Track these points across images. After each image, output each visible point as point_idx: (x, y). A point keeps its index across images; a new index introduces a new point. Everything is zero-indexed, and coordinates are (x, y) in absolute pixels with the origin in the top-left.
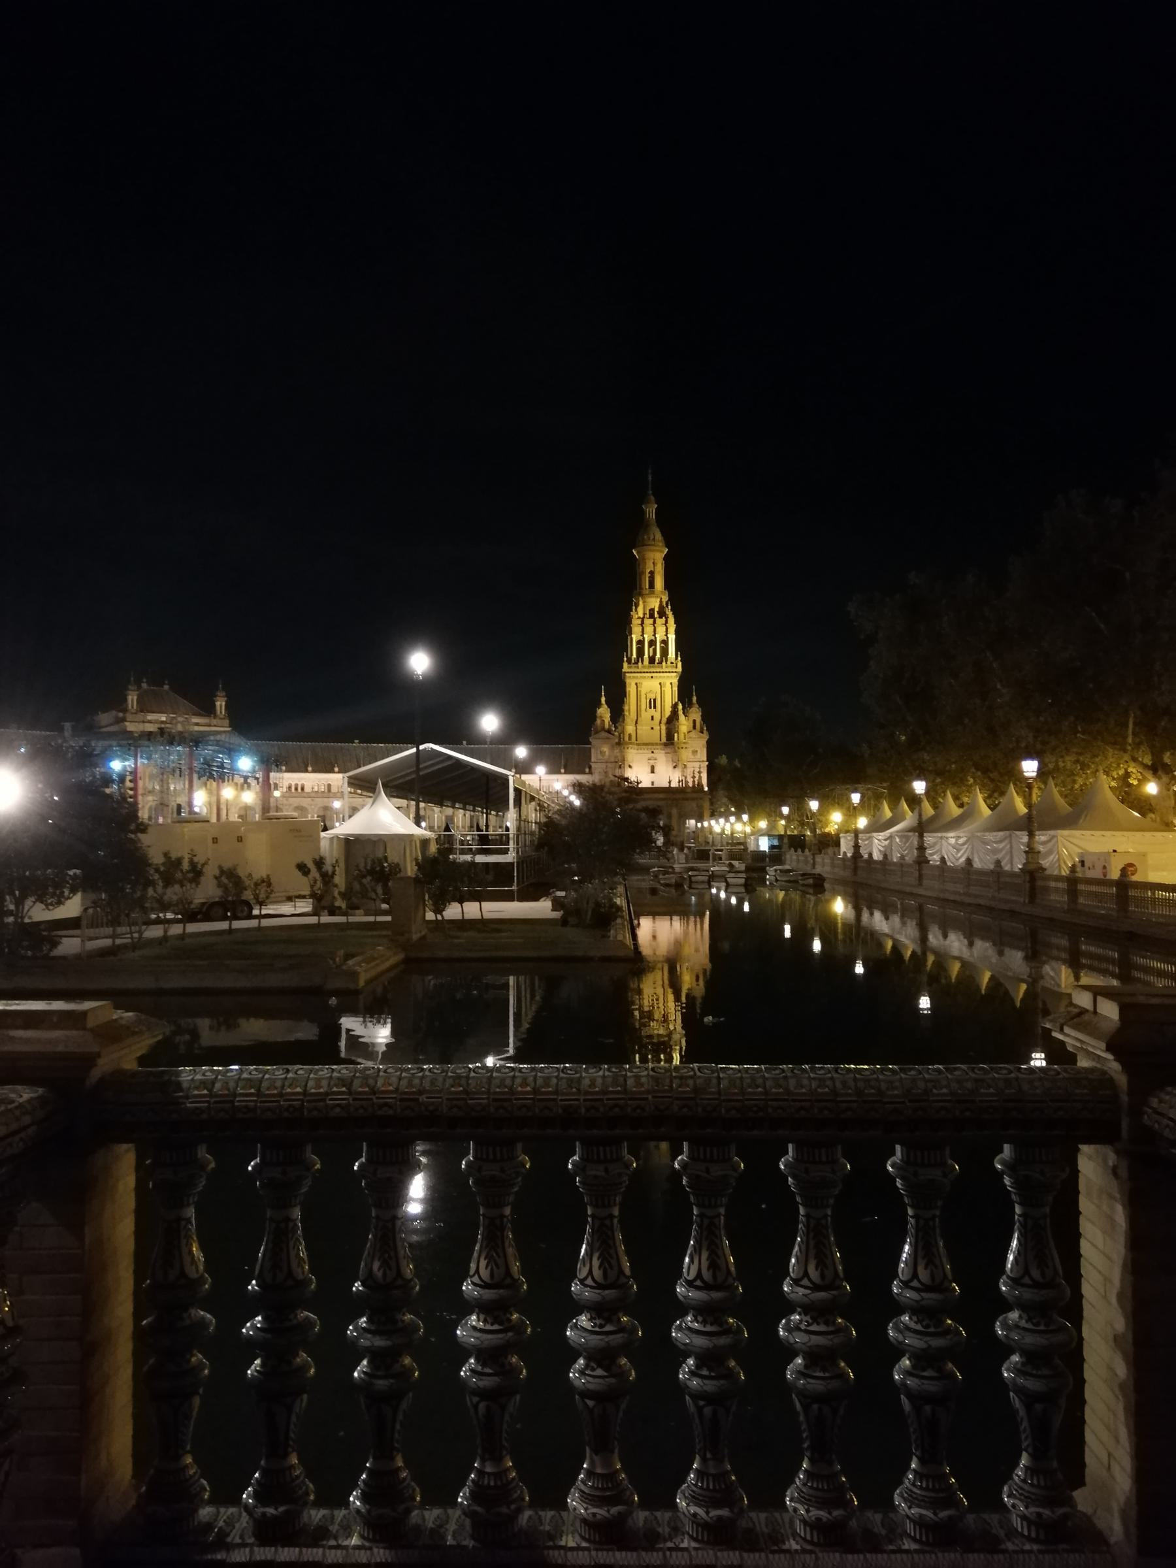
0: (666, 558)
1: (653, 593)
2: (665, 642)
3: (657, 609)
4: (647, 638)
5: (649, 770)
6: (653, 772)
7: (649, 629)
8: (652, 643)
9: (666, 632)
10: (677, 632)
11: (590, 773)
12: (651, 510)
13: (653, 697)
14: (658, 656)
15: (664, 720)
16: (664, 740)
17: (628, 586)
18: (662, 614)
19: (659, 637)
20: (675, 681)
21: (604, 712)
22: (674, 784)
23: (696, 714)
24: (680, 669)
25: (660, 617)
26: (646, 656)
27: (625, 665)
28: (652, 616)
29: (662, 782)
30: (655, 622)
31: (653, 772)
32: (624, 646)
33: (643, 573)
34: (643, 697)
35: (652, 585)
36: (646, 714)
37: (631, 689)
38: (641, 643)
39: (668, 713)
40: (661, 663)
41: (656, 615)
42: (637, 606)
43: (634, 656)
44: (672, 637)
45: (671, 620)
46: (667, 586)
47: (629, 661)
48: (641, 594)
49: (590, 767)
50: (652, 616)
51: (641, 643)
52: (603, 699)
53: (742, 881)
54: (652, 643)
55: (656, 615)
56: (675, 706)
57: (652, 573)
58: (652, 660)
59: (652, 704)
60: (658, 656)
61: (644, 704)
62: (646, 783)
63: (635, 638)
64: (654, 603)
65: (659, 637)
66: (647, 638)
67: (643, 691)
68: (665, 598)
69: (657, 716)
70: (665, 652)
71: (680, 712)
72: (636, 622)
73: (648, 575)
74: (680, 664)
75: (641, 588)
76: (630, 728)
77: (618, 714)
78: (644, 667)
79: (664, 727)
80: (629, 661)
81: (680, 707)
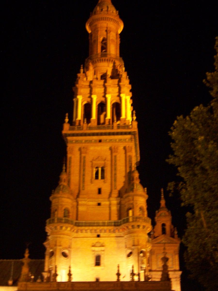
5: (92, 261)
6: (98, 263)
7: (98, 90)
8: (102, 107)
13: (100, 163)
16: (115, 218)
18: (116, 75)
22: (126, 278)
27: (66, 126)
29: (107, 274)
31: (98, 263)
33: (96, 41)
34: (88, 164)
38: (88, 108)
42: (86, 68)
47: (71, 123)
51: (88, 108)
56: (129, 177)
61: (90, 173)
67: (89, 158)
69: (106, 187)
79: (114, 202)
80: (71, 123)
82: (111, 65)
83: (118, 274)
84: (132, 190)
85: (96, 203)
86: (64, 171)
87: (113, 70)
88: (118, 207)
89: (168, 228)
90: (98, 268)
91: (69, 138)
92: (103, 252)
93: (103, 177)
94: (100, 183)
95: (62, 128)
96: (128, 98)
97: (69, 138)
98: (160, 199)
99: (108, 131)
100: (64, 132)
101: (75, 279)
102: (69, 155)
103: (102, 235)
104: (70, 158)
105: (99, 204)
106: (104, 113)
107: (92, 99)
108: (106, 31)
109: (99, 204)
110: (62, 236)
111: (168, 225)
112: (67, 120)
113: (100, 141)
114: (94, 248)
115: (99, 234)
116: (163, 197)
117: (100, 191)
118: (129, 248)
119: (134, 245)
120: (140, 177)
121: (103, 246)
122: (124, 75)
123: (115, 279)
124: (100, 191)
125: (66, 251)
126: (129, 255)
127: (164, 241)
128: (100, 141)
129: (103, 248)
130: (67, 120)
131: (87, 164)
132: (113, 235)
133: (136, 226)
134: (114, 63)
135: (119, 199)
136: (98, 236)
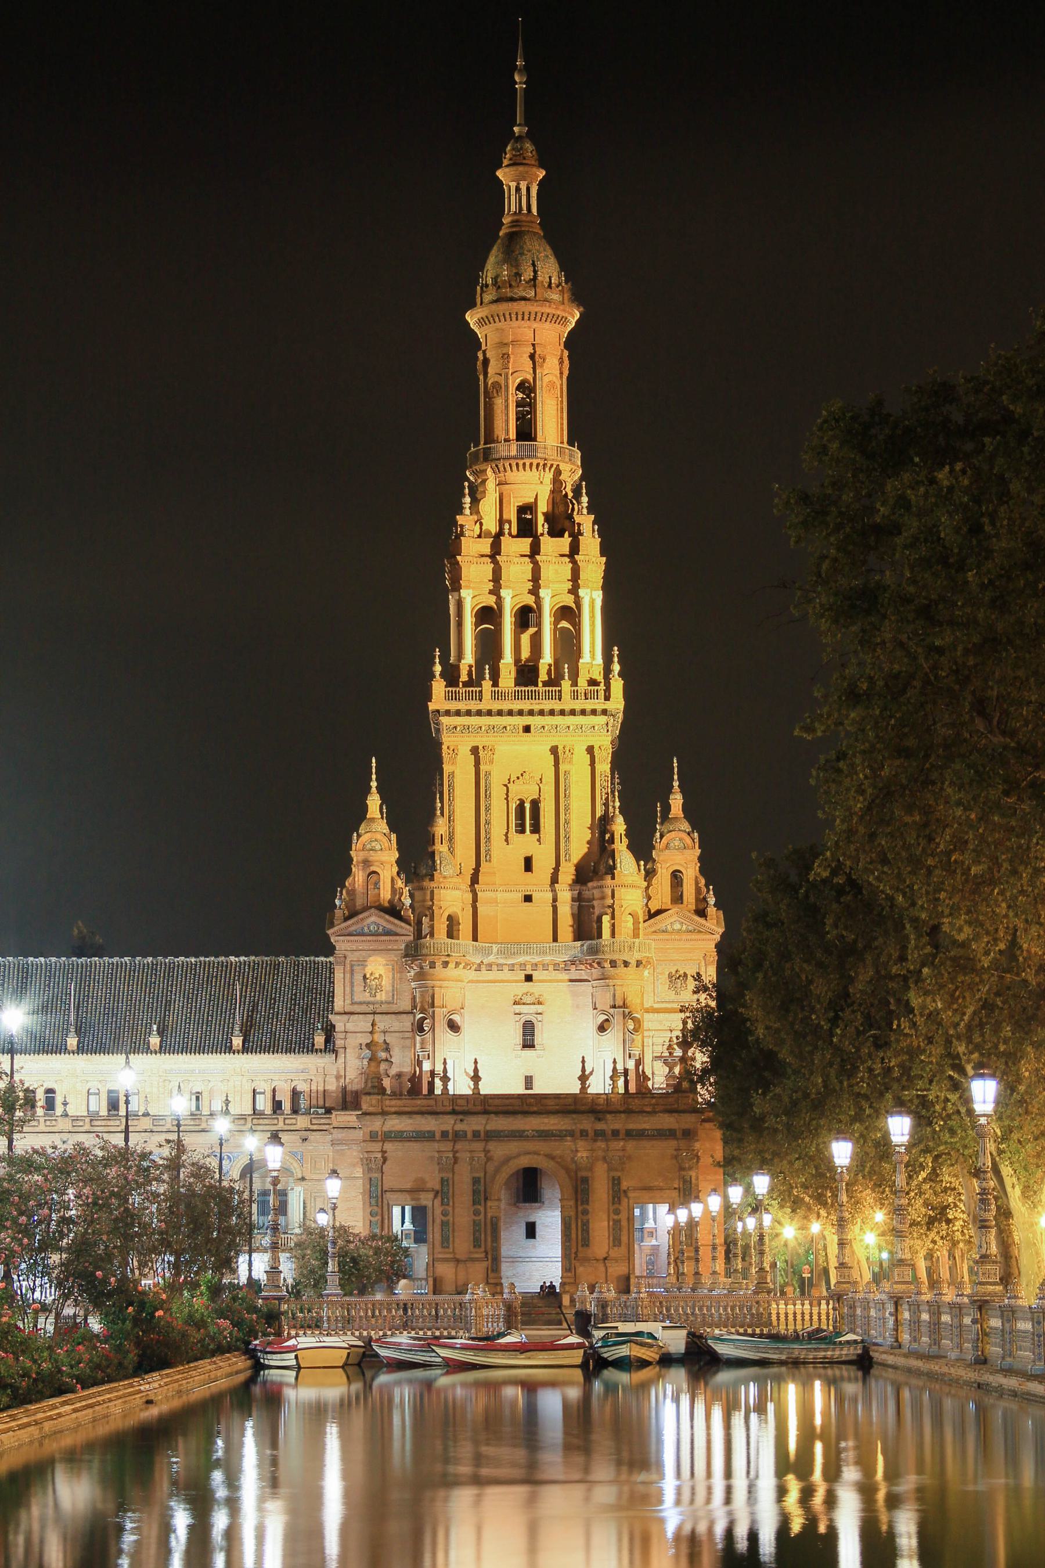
0: (572, 342)
1: (532, 454)
2: (569, 613)
3: (543, 507)
4: (511, 601)
6: (528, 1044)
8: (526, 617)
9: (574, 579)
10: (609, 585)
11: (330, 1046)
12: (520, 185)
13: (526, 791)
14: (547, 658)
15: (567, 874)
17: (446, 428)
18: (560, 523)
19: (553, 595)
20: (605, 742)
21: (375, 846)
22: (599, 1085)
23: (679, 850)
24: (617, 702)
25: (555, 532)
26: (508, 658)
27: (439, 687)
28: (527, 528)
29: (556, 1078)
30: (535, 549)
31: (528, 1044)
32: (437, 628)
34: (497, 793)
35: (526, 432)
36: (507, 851)
37: (458, 768)
38: (488, 615)
39: (579, 844)
40: (554, 681)
41: (542, 526)
43: (469, 658)
44: (592, 598)
45: (591, 543)
46: (577, 432)
47: (451, 677)
48: (487, 456)
49: (329, 1031)
50: (527, 528)
51: (488, 615)
52: (374, 802)
53: (579, 1361)
54: (526, 617)
55: (542, 526)
56: (602, 825)
57: (527, 388)
58: (527, 674)
59: (527, 817)
60: (547, 658)
62: (502, 1079)
63: (472, 595)
64: (532, 486)
65: (553, 595)
66: (511, 601)
67: (497, 775)
68: (572, 472)
70: (569, 646)
71: (621, 846)
72: (472, 549)
73: (514, 396)
74: (617, 686)
75: (490, 438)
76: (450, 896)
77: (417, 858)
78: (496, 696)
79: (565, 895)
81: (619, 826)
82: (549, 476)
83: (583, 1078)
84: (611, 870)
85: (520, 896)
86: (438, 812)
87: (553, 492)
88: (576, 908)
89: (689, 890)
90: (528, 1052)
91: (445, 720)
92: (539, 1017)
93: (536, 829)
94: (526, 843)
95: (429, 697)
96: (598, 596)
97: (445, 720)
98: (669, 789)
99: (547, 705)
100: (432, 706)
101: (485, 1089)
102: (447, 768)
103: (536, 975)
104: (452, 775)
105: (528, 899)
106: (532, 630)
107: (499, 600)
108: (532, 357)
109: (528, 899)
110: (445, 984)
111: (691, 872)
112: (438, 668)
113: (527, 729)
114: (518, 1008)
115: (530, 972)
116: (676, 784)
117: (528, 864)
118: (603, 1012)
119: (614, 1007)
120: (629, 834)
121: (540, 1003)
122: (585, 521)
123: (575, 1088)
124: (528, 864)
125: (456, 1018)
126: (602, 1028)
127: (677, 926)
128: (527, 729)
129: (539, 1008)
130: (438, 668)
131: (494, 794)
132: (565, 976)
133: (620, 963)
134: (558, 472)
135: (578, 887)
136: (529, 978)
